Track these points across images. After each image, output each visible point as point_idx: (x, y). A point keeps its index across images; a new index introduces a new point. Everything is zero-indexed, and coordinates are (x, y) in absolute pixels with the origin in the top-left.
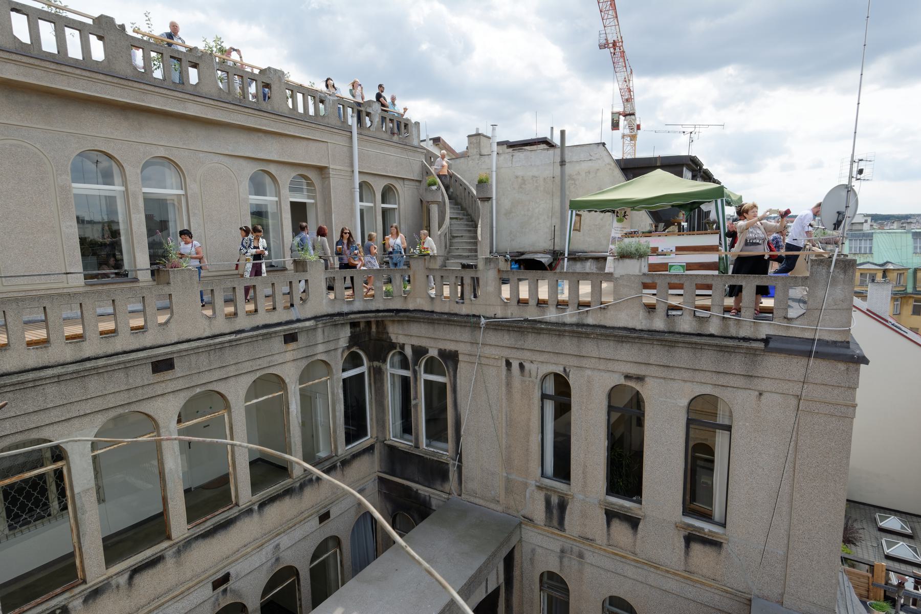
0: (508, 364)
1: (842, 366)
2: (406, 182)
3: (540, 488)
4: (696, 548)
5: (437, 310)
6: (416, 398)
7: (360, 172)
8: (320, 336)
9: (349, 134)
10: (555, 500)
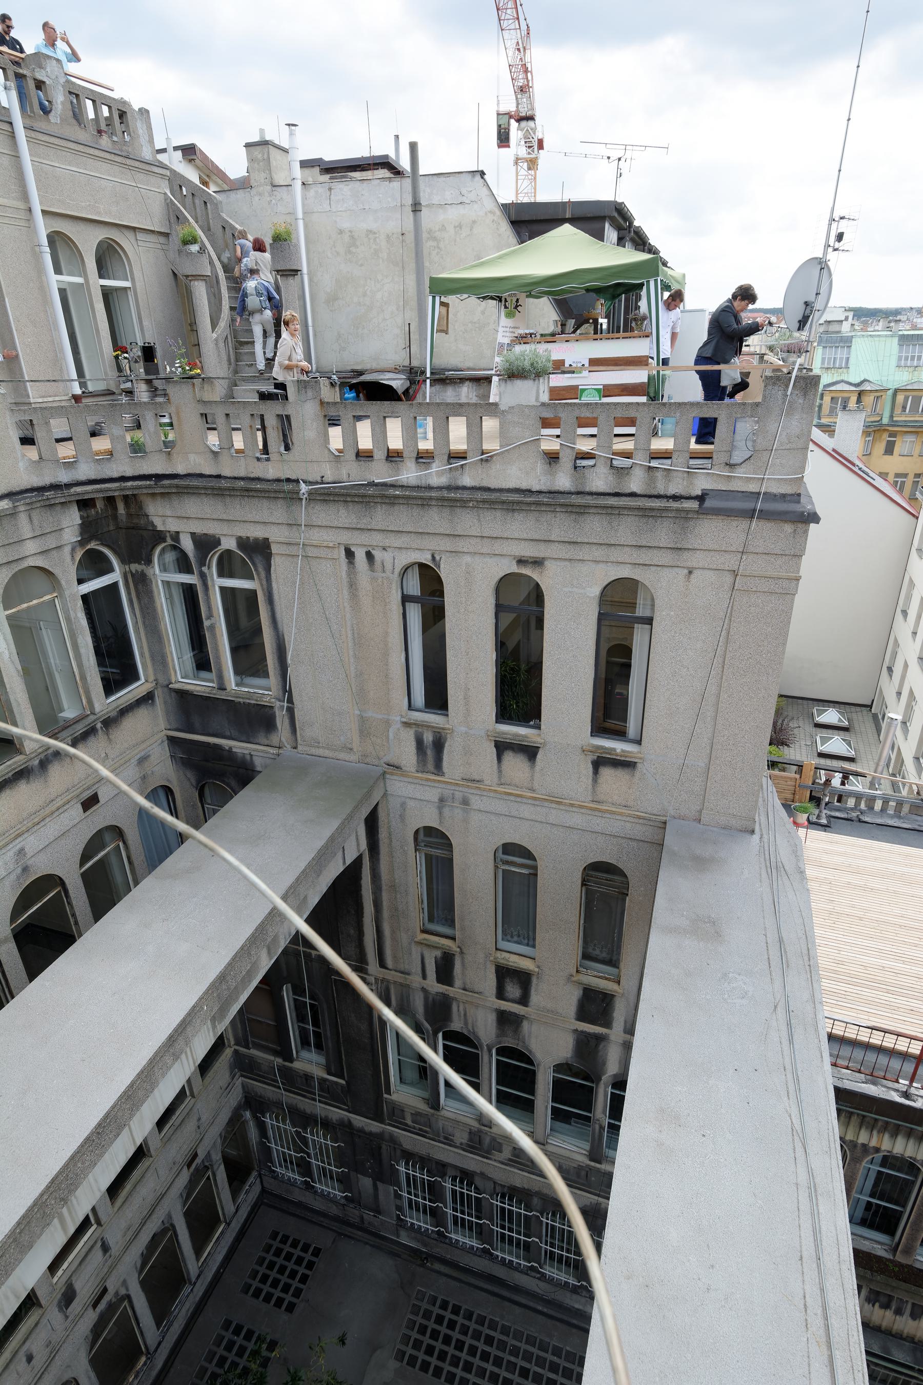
0: (350, 554)
1: (788, 528)
2: (140, 236)
3: (407, 724)
4: (607, 773)
5: (227, 472)
6: (210, 616)
7: (43, 211)
9: (6, 127)
10: (428, 737)
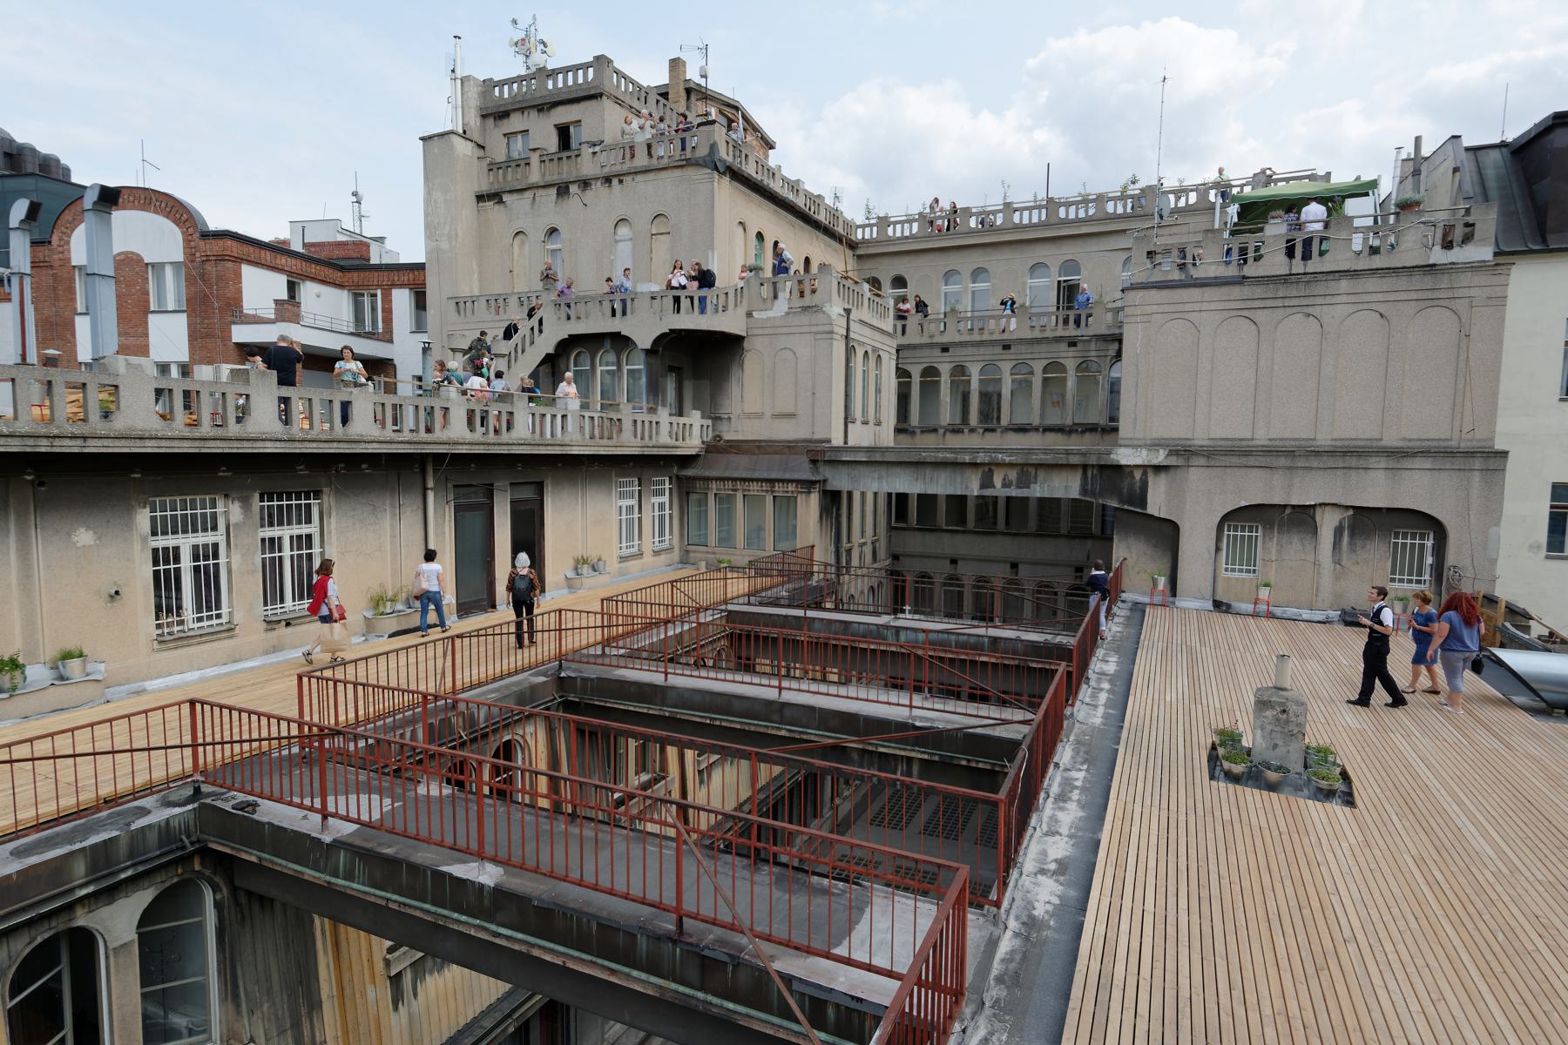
8: (1093, 346)
